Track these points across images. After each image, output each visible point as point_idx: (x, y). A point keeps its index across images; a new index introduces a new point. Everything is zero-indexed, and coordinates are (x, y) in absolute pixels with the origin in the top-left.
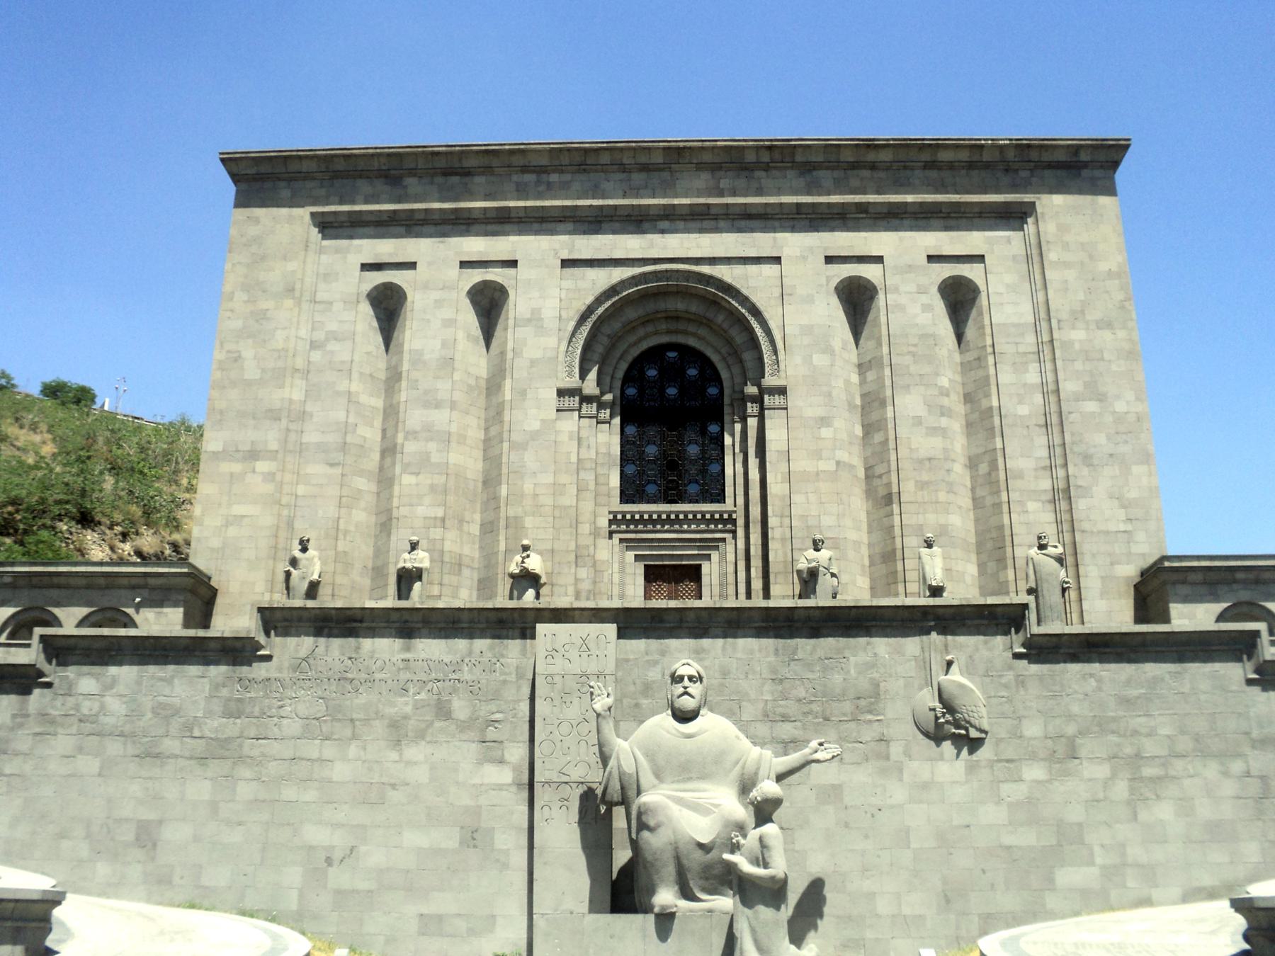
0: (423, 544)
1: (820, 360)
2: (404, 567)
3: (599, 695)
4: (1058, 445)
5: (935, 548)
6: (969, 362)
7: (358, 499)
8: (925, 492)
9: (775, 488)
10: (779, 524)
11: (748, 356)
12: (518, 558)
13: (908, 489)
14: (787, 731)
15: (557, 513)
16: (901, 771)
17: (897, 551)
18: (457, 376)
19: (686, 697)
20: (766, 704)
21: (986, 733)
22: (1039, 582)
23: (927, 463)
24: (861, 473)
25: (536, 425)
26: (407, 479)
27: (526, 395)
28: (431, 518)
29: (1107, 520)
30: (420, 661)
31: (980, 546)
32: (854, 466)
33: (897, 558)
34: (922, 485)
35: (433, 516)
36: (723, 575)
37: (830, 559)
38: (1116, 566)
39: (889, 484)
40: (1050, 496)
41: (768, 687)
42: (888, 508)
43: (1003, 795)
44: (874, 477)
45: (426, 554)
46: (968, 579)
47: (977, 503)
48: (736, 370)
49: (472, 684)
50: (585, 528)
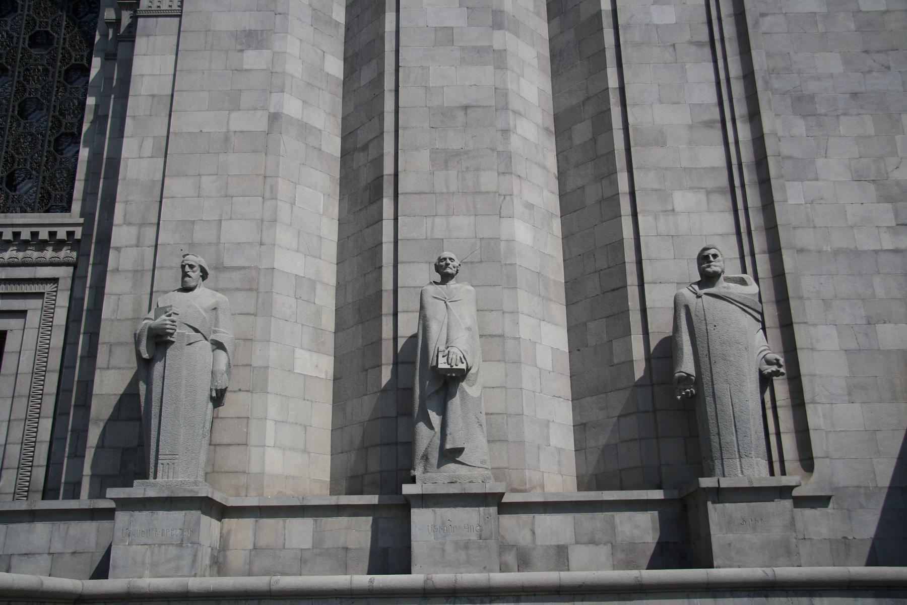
5: (452, 284)
8: (453, 173)
10: (133, 242)
22: (704, 360)
23: (460, 114)
24: (333, 145)
29: (852, 227)
31: (572, 286)
32: (320, 130)
33: (384, 311)
36: (42, 352)
37: (215, 309)
38: (880, 327)
39: (379, 160)
40: (725, 182)
42: (374, 207)
46: (544, 359)
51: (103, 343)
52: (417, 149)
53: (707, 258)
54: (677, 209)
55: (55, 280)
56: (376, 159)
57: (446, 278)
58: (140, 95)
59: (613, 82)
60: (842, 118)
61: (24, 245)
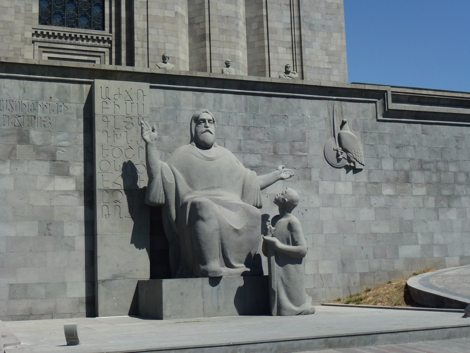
3: (147, 130)
4: (295, 17)
5: (230, 68)
9: (139, 23)
10: (141, 46)
13: (215, 33)
14: (254, 160)
16: (317, 187)
17: (208, 68)
19: (208, 133)
20: (240, 143)
21: (364, 165)
23: (226, 19)
24: (187, 21)
29: (319, 61)
30: (5, 102)
34: (223, 31)
39: (204, 29)
40: (291, 45)
41: (241, 131)
42: (203, 43)
43: (372, 203)
47: (250, 45)
49: (45, 120)
50: (18, 37)
52: (215, 28)
53: (288, 67)
54: (279, 52)
55: (104, 52)
56: (202, 28)
57: (228, 66)
59: (265, 13)
60: (320, 32)
61: (94, 40)
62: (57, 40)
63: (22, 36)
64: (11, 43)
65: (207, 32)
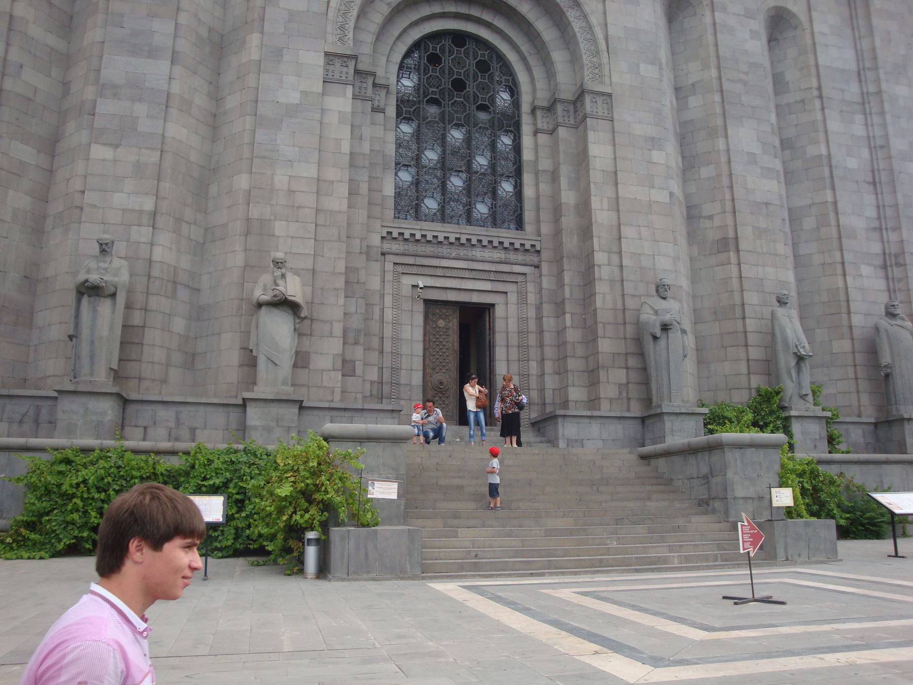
0: (120, 248)
1: (648, 71)
2: (87, 281)
6: (788, 104)
7: (20, 176)
9: (602, 215)
10: (606, 262)
11: (558, 57)
12: (266, 278)
15: (321, 221)
18: (183, 18)
25: (294, 98)
26: (99, 152)
27: (282, 56)
28: (133, 211)
35: (137, 208)
36: (522, 320)
40: (880, 262)
42: (723, 256)
44: (700, 217)
45: (125, 263)
48: (538, 72)
51: (600, 322)
54: (864, 274)
58: (596, 169)
62: (429, 249)
63: (361, 242)
64: (339, 258)
65: (731, 234)
